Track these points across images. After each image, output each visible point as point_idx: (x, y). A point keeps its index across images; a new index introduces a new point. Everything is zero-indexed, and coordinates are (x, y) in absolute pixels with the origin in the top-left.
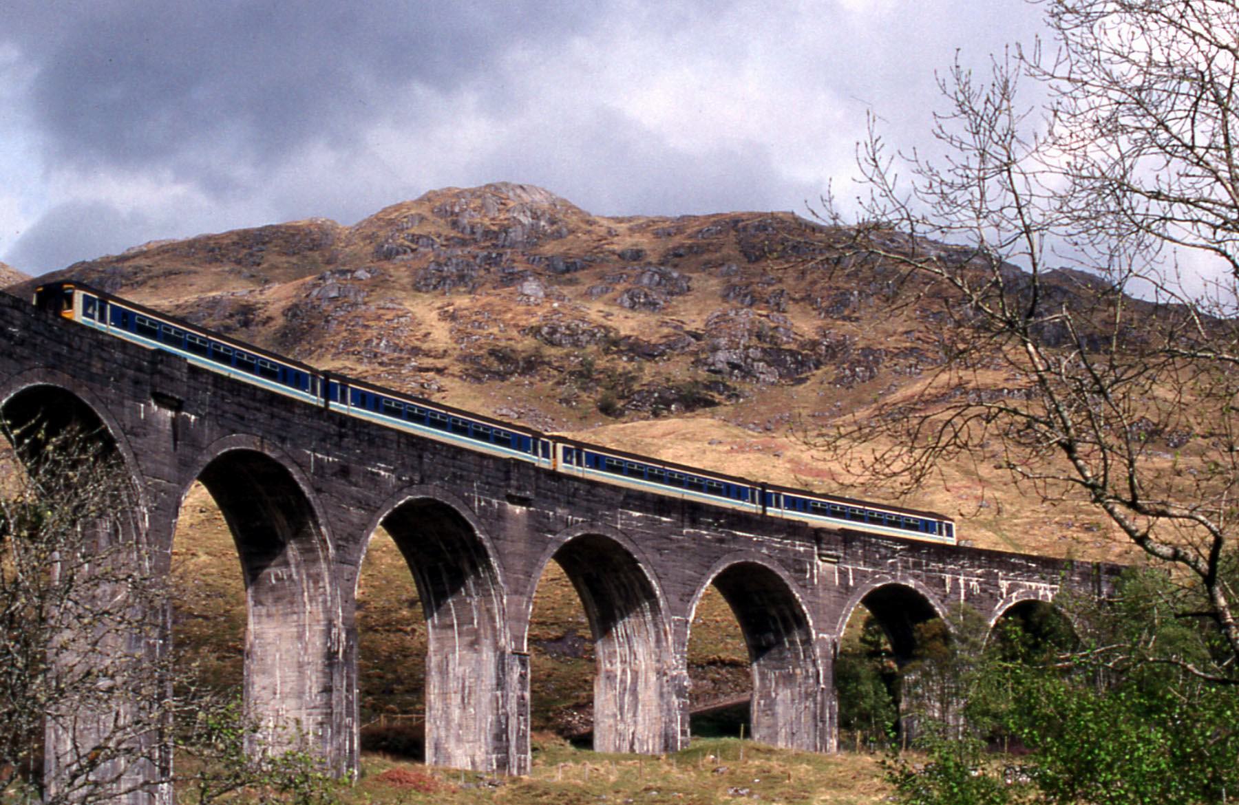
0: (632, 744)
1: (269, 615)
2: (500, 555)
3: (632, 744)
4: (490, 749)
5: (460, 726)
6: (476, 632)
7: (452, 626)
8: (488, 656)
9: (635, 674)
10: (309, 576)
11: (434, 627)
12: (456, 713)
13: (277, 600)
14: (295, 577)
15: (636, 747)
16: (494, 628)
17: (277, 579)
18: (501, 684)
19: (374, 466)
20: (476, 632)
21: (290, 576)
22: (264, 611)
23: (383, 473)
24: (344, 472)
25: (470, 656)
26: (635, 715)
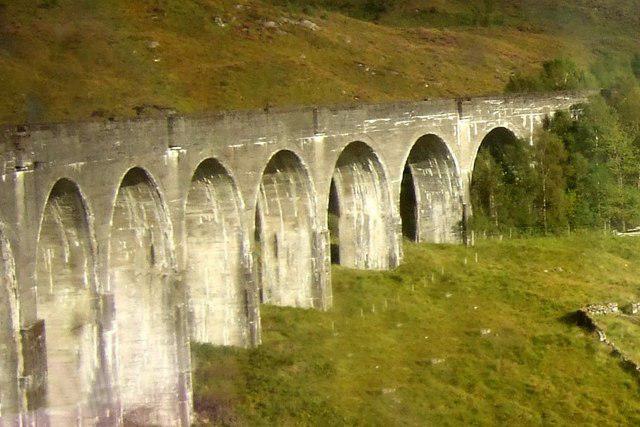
0: (366, 263)
1: (199, 243)
2: (313, 175)
3: (366, 263)
4: (309, 294)
5: (287, 279)
6: (296, 219)
7: (279, 215)
8: (304, 234)
9: (367, 219)
10: (227, 220)
11: (265, 215)
12: (283, 271)
13: (204, 233)
14: (217, 220)
15: (369, 264)
16: (309, 218)
17: (204, 221)
18: (314, 253)
19: (257, 141)
20: (296, 219)
21: (213, 220)
22: (194, 240)
23: (262, 143)
24: (245, 149)
25: (292, 234)
26: (368, 243)
